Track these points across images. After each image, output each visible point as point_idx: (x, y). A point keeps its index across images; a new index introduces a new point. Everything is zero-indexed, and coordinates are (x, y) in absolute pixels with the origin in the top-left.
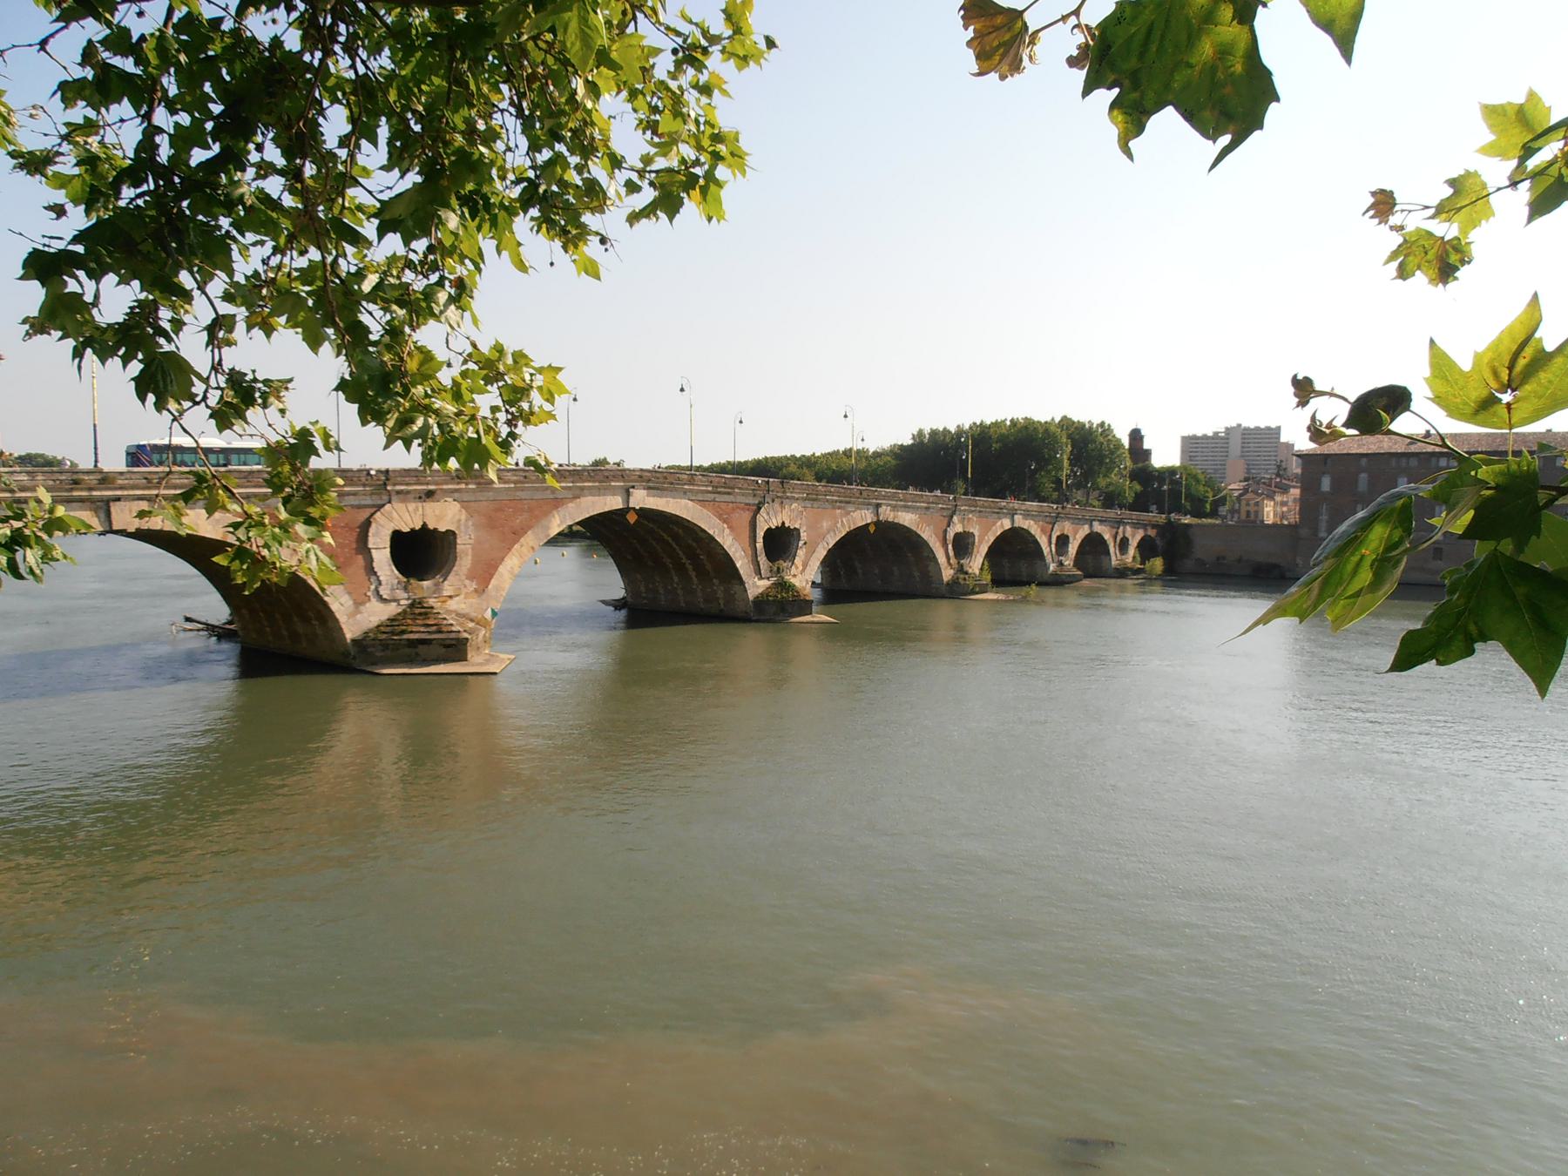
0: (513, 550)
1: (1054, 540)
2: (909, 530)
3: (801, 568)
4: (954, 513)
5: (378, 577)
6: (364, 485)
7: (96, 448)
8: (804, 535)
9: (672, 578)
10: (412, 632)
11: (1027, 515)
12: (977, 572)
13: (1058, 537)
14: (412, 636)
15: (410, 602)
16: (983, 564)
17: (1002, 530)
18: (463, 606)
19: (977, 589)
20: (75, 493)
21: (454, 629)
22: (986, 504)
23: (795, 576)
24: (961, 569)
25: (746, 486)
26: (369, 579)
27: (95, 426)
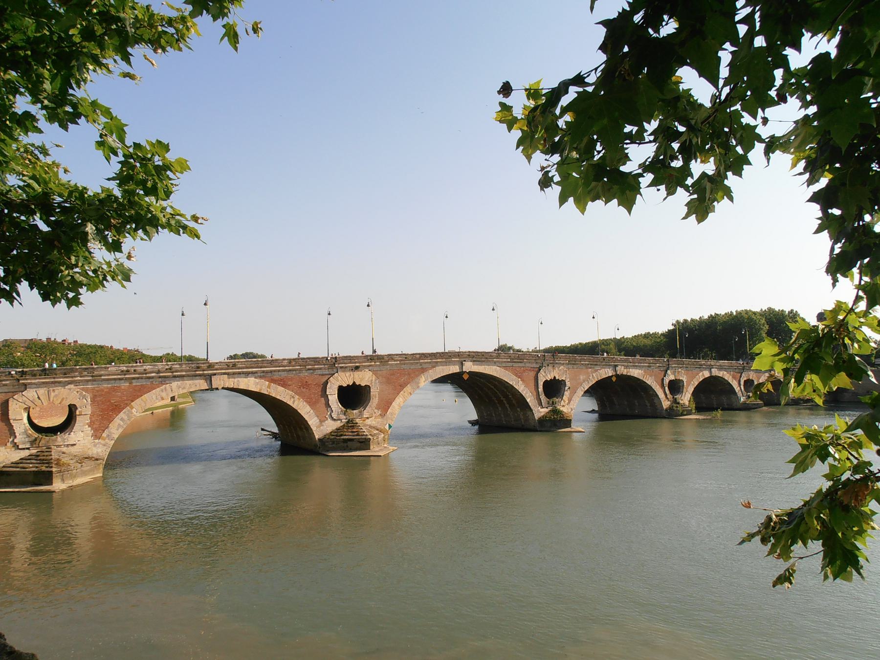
0: (400, 394)
1: (742, 383)
2: (639, 379)
3: (567, 401)
4: (668, 369)
5: (331, 408)
6: (324, 365)
7: (207, 352)
8: (568, 384)
9: (498, 408)
10: (345, 435)
11: (721, 368)
12: (687, 403)
13: (745, 381)
14: (345, 437)
15: (347, 420)
16: (690, 398)
17: (704, 378)
18: (374, 422)
19: (685, 413)
20: (197, 373)
21: (365, 434)
22: (690, 363)
23: (563, 406)
24: (675, 401)
25: (531, 358)
26: (327, 410)
27: (207, 343)
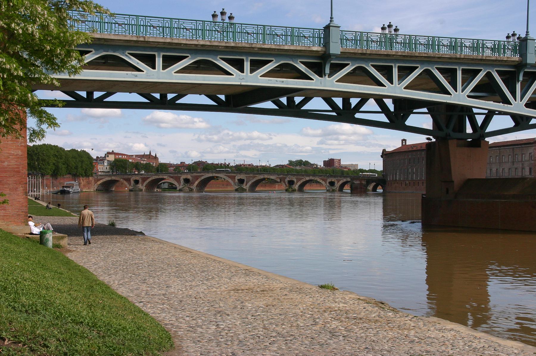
8: (245, 180)
